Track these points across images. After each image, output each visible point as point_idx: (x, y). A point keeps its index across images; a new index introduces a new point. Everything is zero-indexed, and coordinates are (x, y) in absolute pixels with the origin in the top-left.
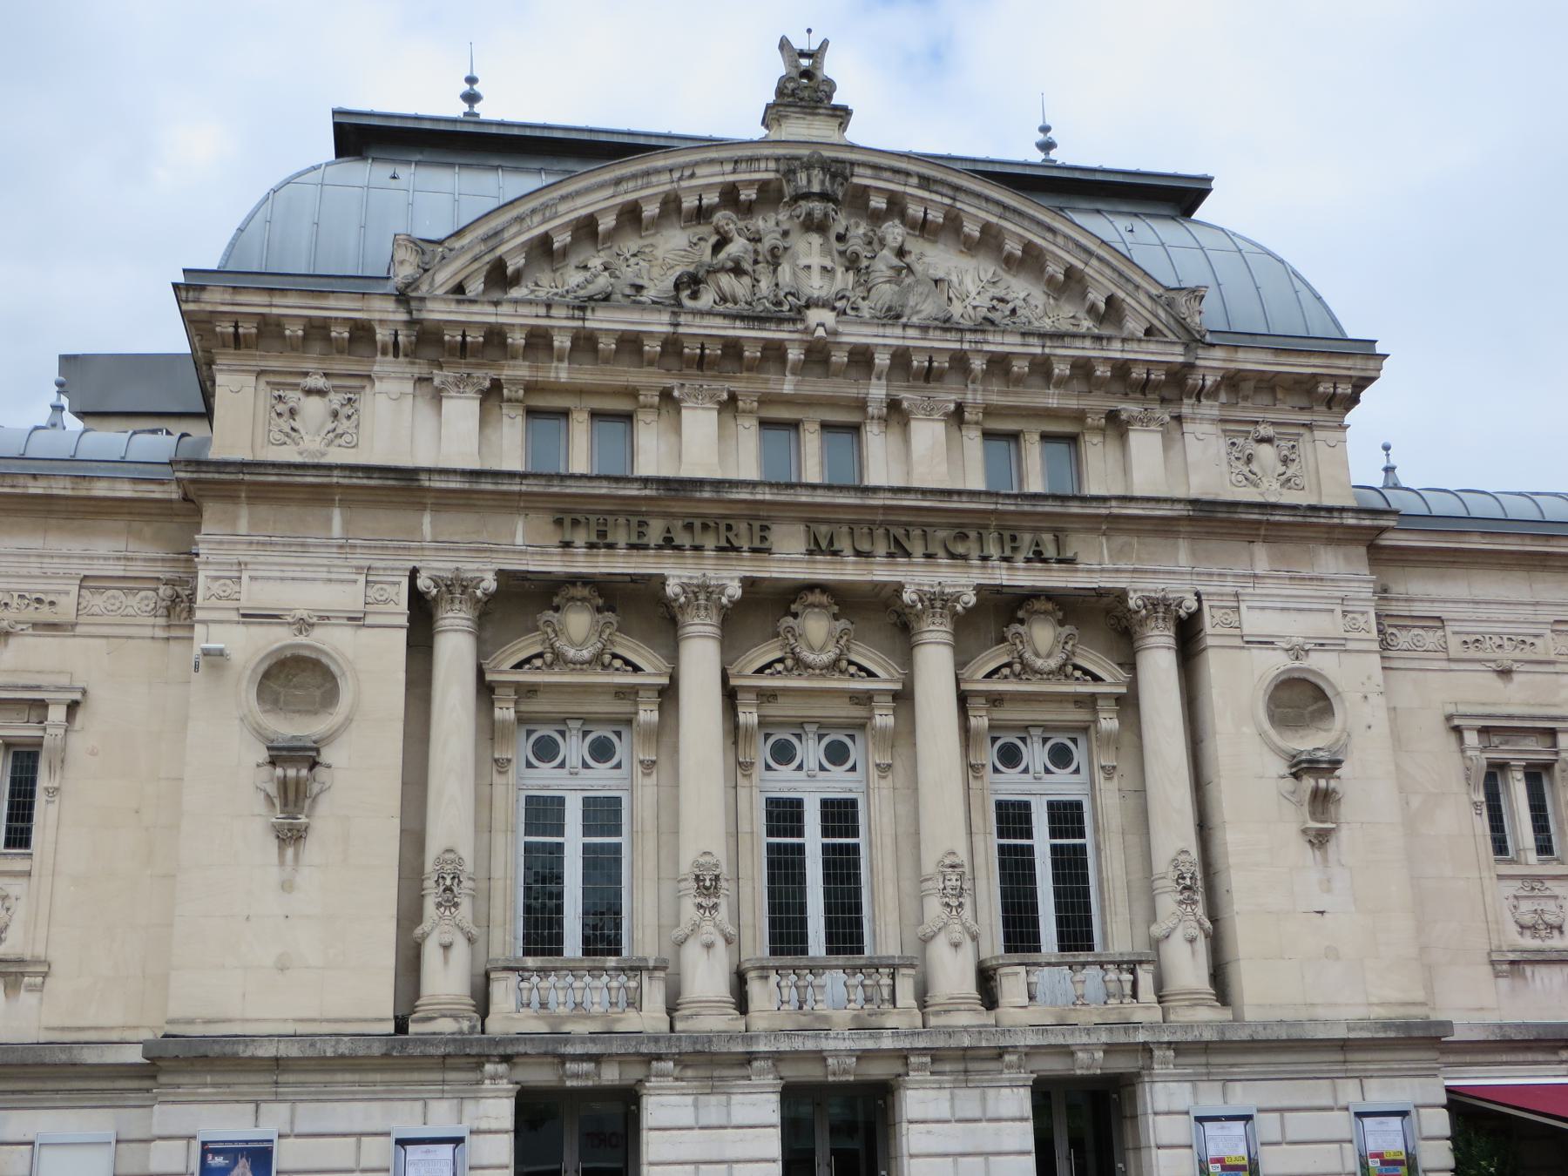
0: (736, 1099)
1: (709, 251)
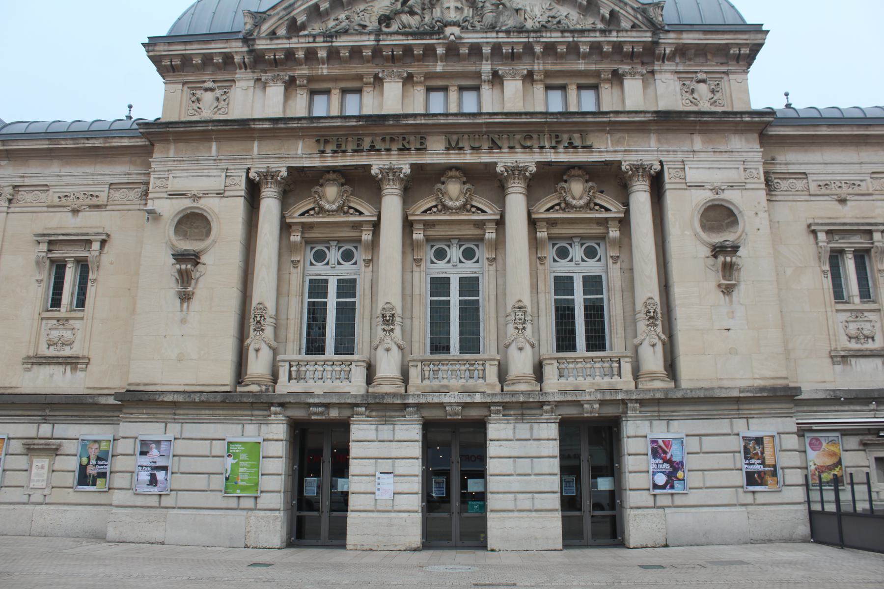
0: (397, 427)
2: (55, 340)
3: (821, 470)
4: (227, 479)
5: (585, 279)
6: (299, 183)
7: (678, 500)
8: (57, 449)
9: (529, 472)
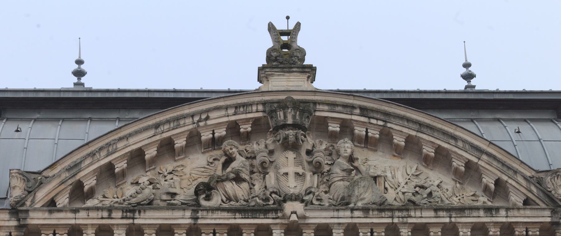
1: (220, 167)
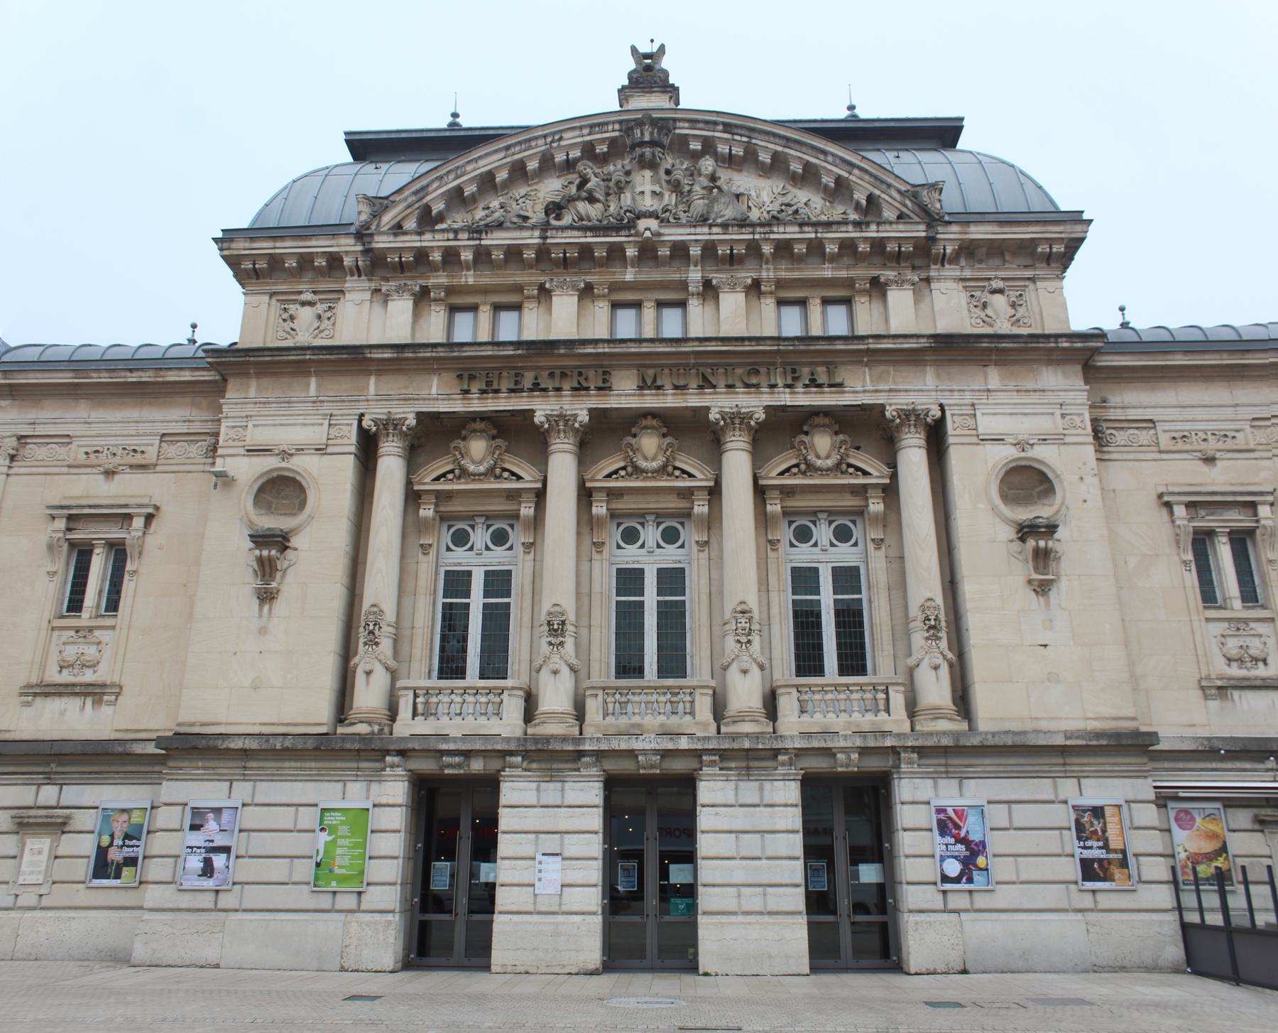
2: (72, 659)
3: (1195, 859)
4: (318, 865)
5: (836, 571)
6: (432, 435)
7: (981, 901)
8: (64, 824)
9: (758, 853)
